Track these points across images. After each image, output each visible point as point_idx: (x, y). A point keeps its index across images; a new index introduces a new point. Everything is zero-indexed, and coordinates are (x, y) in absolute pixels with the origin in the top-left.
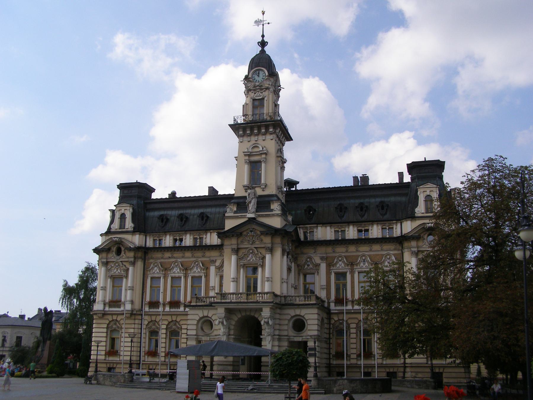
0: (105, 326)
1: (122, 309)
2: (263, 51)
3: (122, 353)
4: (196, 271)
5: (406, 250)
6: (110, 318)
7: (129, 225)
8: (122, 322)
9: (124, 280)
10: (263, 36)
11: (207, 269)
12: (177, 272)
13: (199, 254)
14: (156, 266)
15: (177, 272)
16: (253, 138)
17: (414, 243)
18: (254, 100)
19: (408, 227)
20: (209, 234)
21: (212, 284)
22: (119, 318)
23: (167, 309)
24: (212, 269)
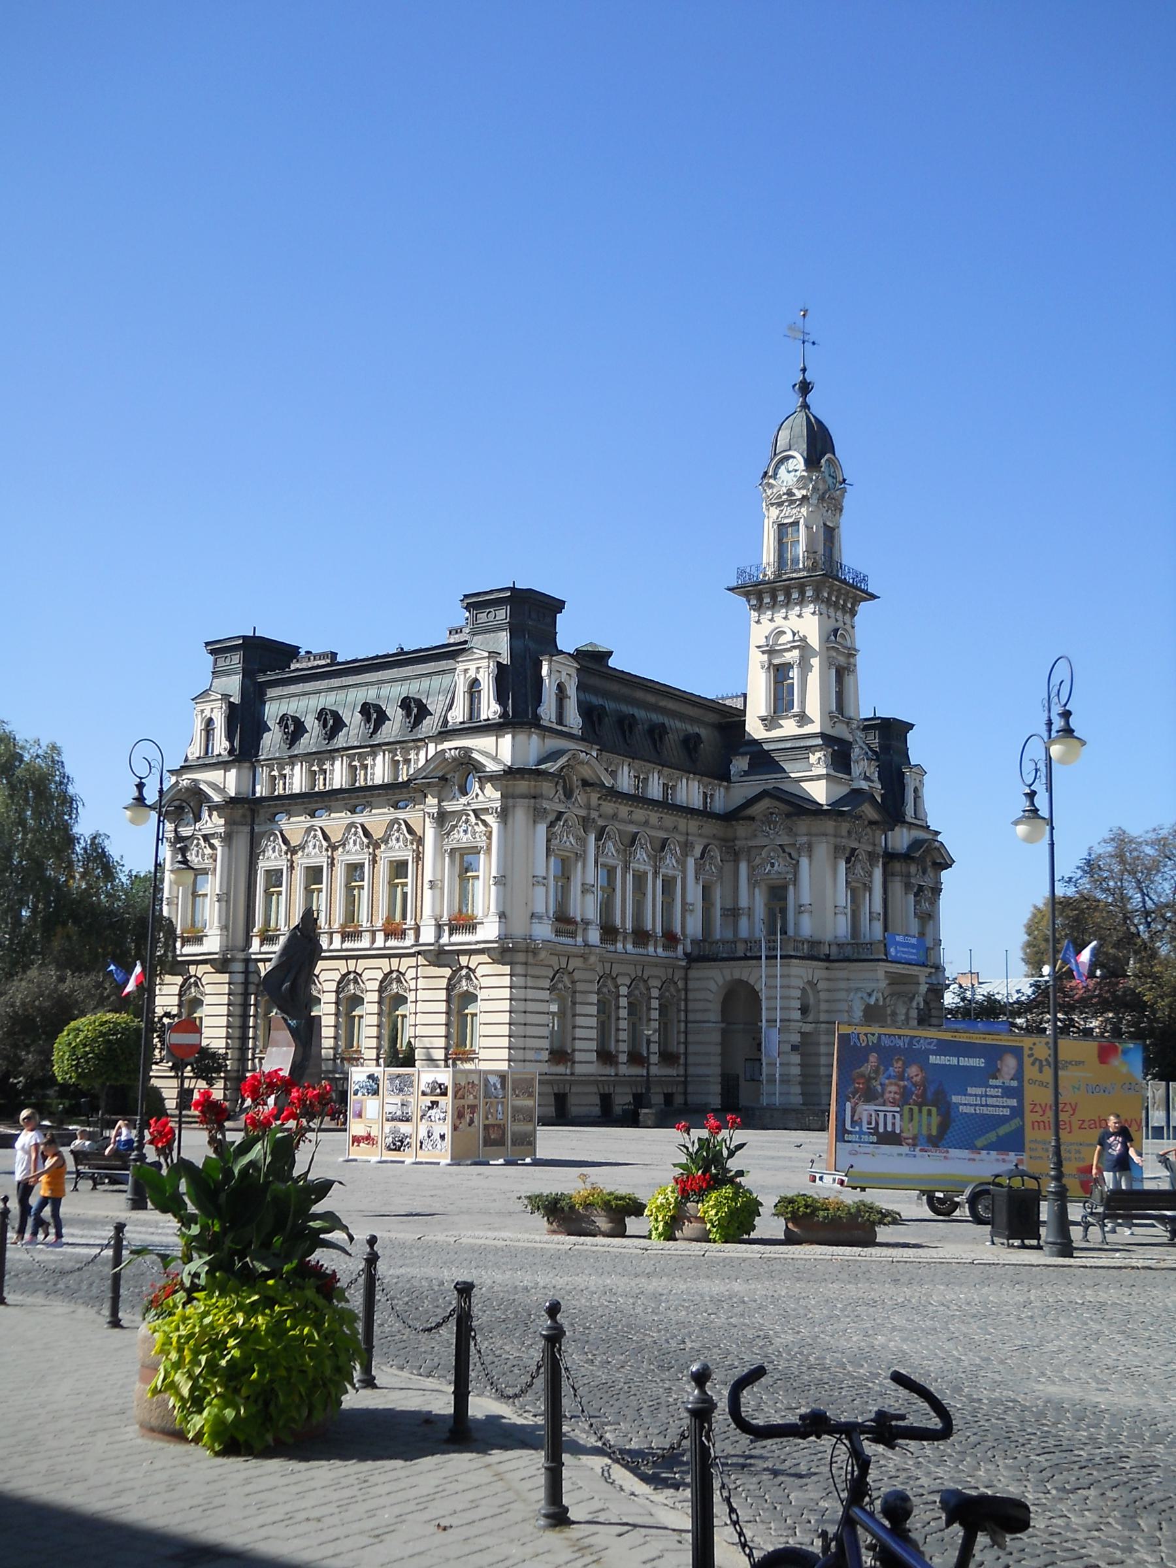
0: (547, 984)
1: (579, 939)
2: (805, 406)
3: (578, 1056)
4: (670, 864)
5: (899, 878)
6: (554, 961)
7: (574, 720)
8: (577, 975)
9: (580, 864)
10: (804, 370)
11: (683, 864)
12: (641, 860)
13: (669, 820)
14: (610, 838)
15: (641, 860)
16: (831, 610)
17: (913, 869)
18: (825, 524)
19: (901, 839)
20: (684, 781)
21: (689, 899)
22: (575, 963)
23: (629, 947)
24: (691, 862)
